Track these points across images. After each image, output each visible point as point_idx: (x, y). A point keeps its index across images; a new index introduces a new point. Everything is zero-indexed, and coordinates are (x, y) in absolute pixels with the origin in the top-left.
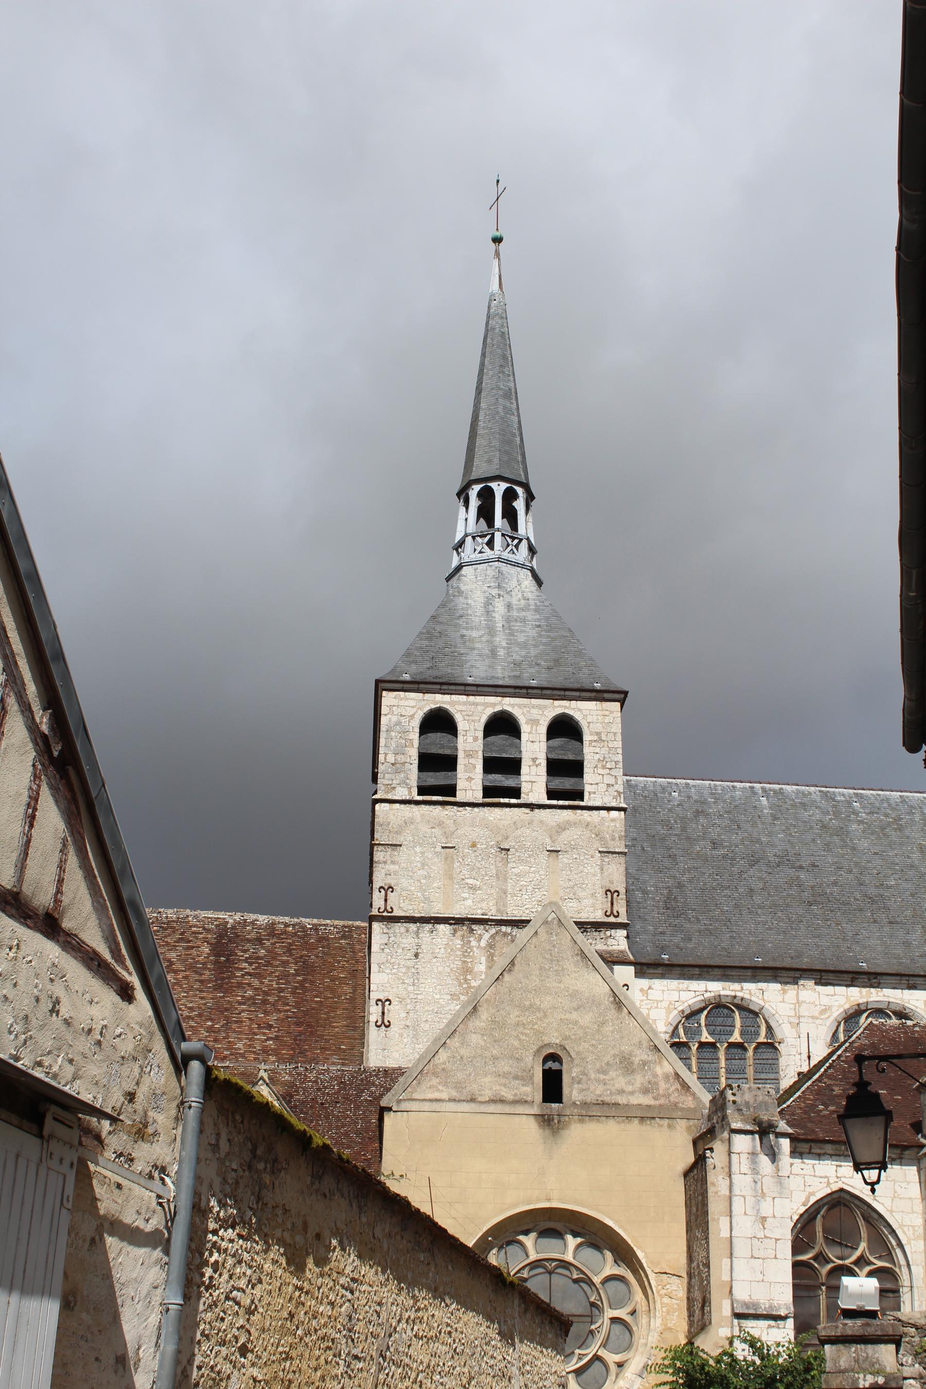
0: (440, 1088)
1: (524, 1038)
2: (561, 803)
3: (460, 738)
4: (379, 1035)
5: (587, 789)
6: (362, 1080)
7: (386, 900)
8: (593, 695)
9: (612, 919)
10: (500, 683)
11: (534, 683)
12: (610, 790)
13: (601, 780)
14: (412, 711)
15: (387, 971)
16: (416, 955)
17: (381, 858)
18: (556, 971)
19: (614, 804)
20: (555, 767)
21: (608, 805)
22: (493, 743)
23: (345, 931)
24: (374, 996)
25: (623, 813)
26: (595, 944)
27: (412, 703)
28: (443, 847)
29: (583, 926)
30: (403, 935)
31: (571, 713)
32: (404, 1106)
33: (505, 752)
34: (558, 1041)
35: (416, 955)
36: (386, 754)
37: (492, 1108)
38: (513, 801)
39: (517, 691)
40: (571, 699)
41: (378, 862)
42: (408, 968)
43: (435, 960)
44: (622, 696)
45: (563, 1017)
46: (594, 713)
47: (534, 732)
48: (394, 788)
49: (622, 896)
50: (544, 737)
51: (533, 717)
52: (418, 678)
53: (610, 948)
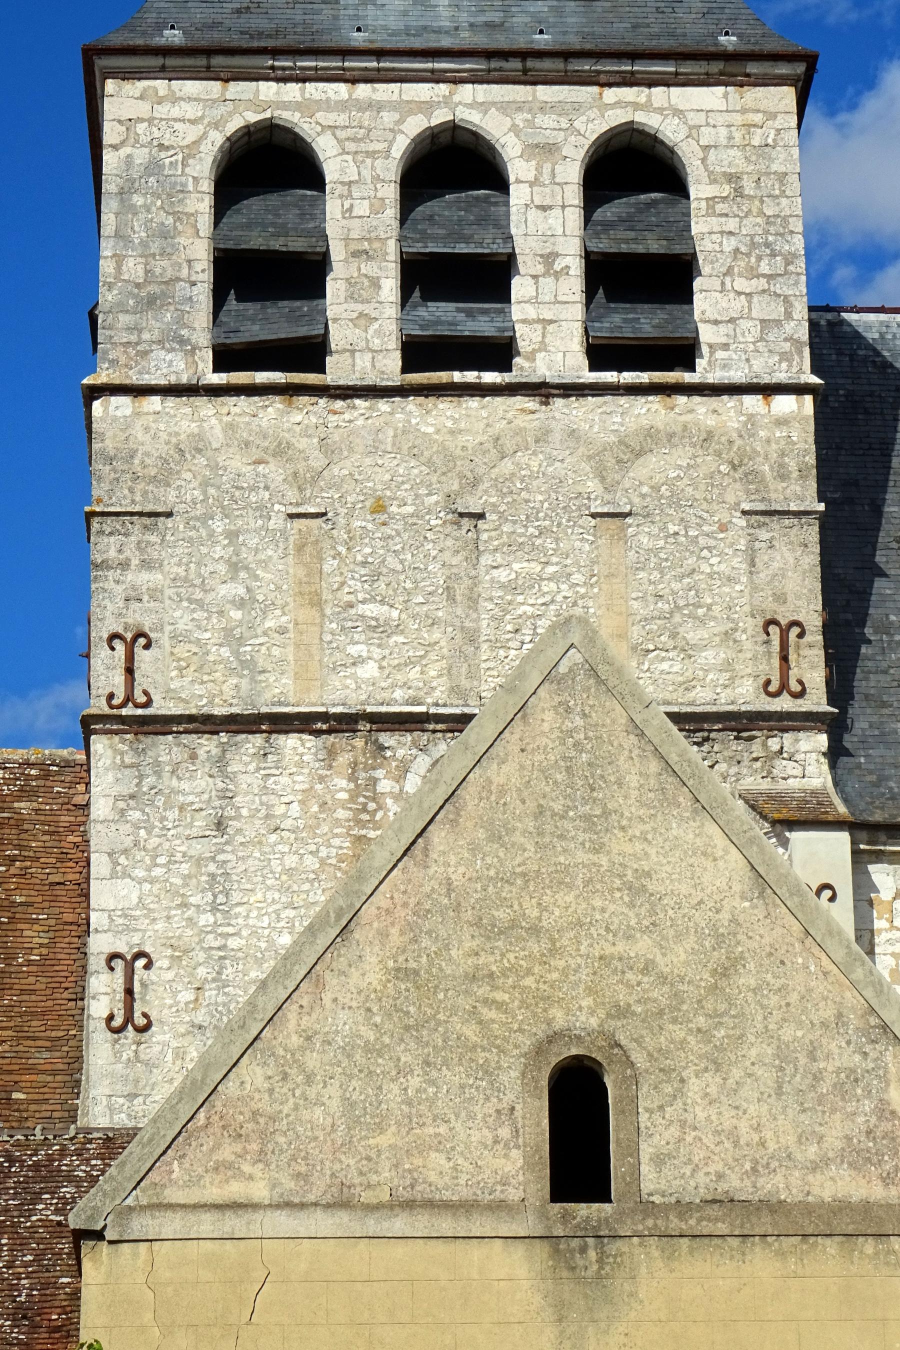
0: (247, 1168)
1: (493, 1014)
2: (628, 377)
3: (333, 207)
4: (117, 1055)
5: (707, 335)
6: (36, 1166)
7: (130, 671)
8: (716, 67)
9: (785, 704)
10: (446, 42)
11: (543, 40)
12: (771, 337)
13: (747, 313)
14: (191, 133)
15: (140, 873)
16: (220, 825)
17: (112, 553)
18: (587, 818)
19: (781, 377)
20: (610, 277)
21: (766, 380)
22: (431, 218)
23: (29, 777)
24: (100, 944)
25: (808, 399)
26: (735, 772)
27: (191, 110)
28: (292, 516)
29: (693, 723)
30: (188, 772)
31: (650, 121)
32: (139, 1225)
33: (467, 240)
34: (594, 1022)
35: (220, 825)
36: (119, 260)
37: (399, 1224)
38: (490, 377)
39: (494, 64)
40: (651, 82)
41: (104, 565)
42: (199, 861)
43: (273, 838)
44: (800, 68)
45: (609, 950)
46: (720, 119)
47: (546, 178)
48: (145, 354)
49: (815, 637)
50: (574, 195)
51: (542, 137)
52: (205, 40)
53: (781, 786)
